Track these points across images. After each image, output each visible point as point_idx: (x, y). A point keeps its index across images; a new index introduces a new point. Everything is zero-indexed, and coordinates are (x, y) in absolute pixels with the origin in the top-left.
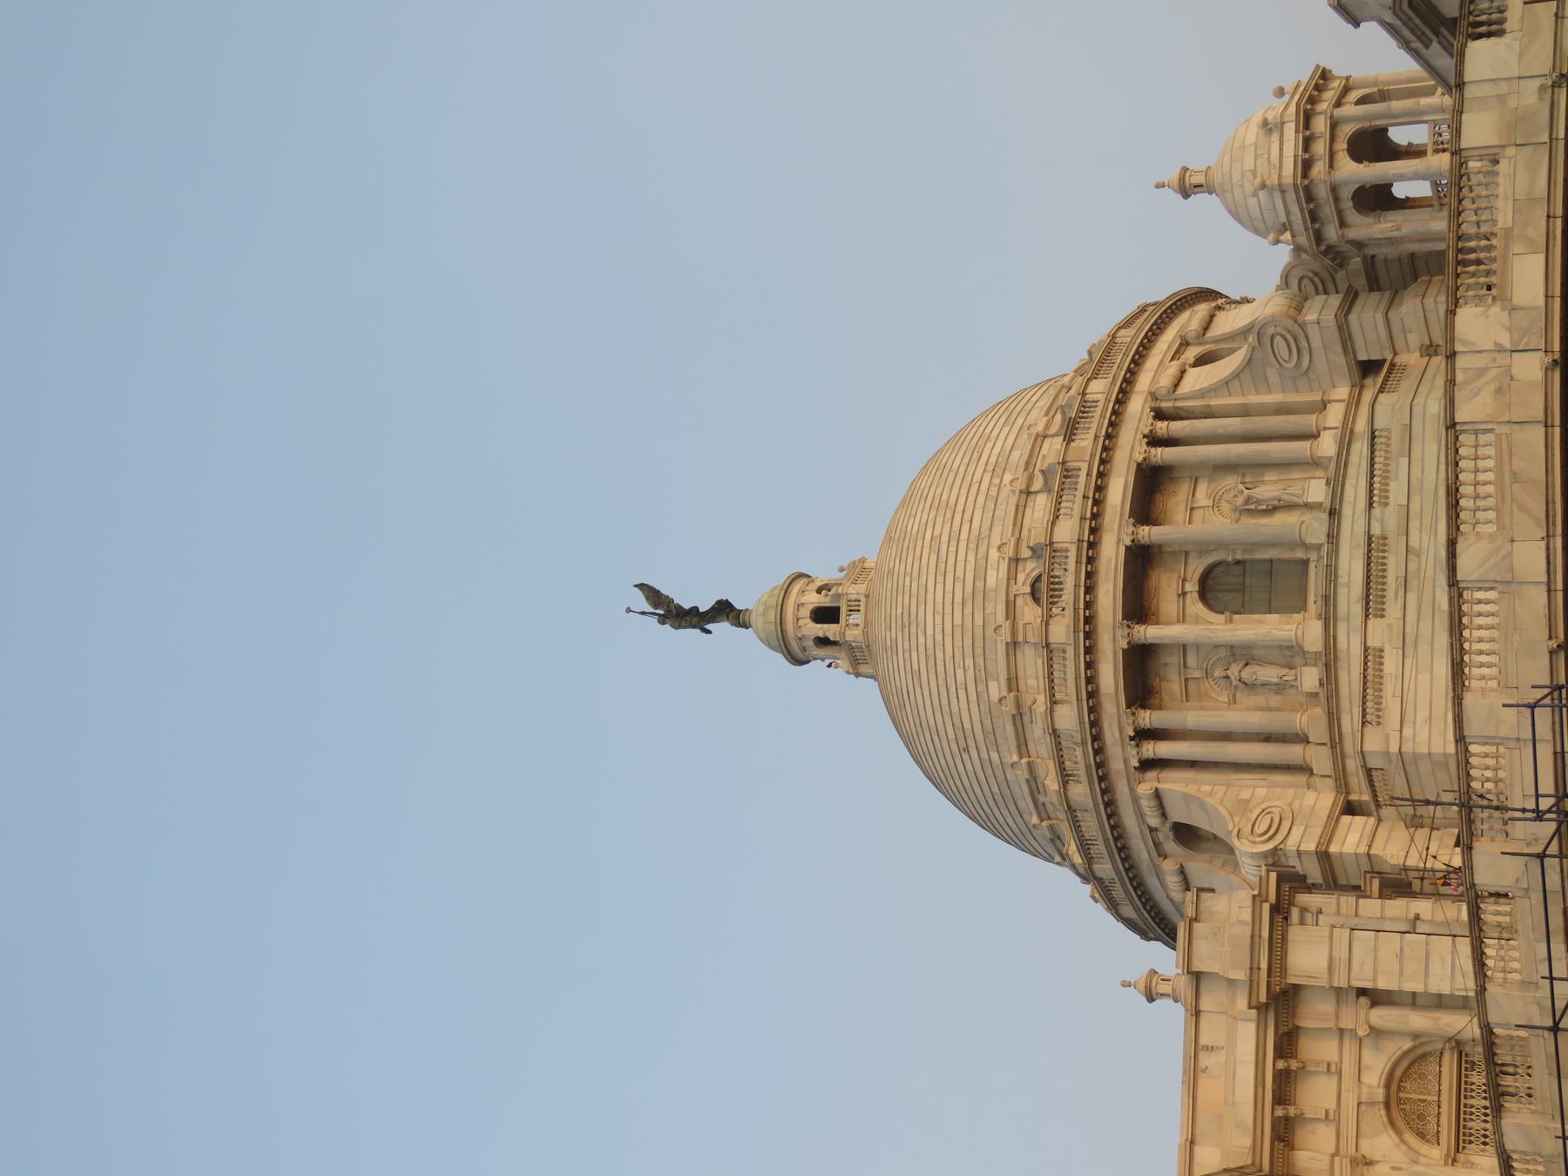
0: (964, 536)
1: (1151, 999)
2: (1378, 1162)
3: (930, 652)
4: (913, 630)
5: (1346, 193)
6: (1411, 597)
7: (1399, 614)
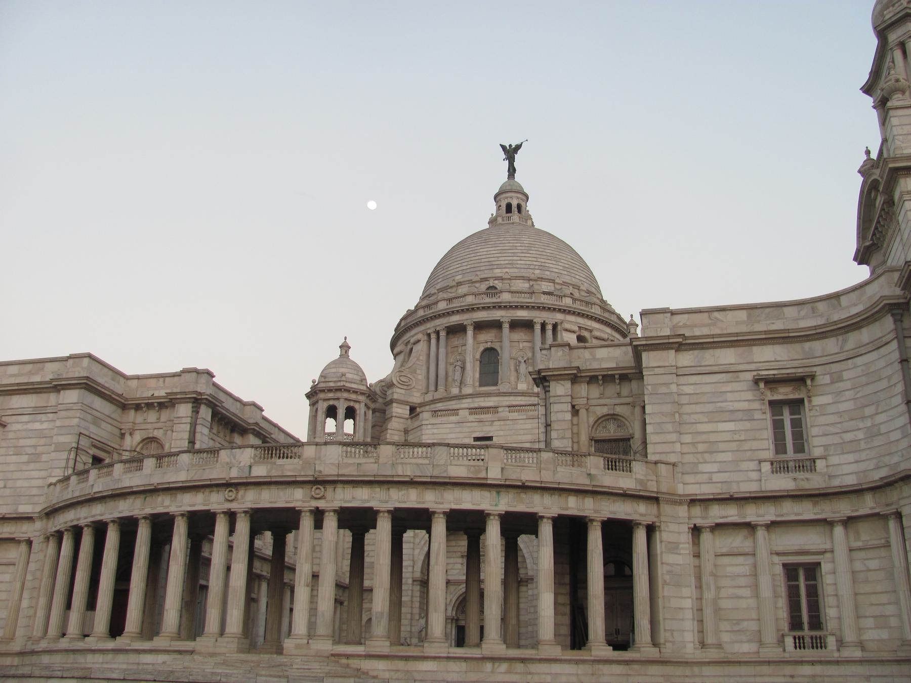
0: (515, 258)
1: (340, 347)
2: (132, 437)
3: (474, 252)
4: (483, 244)
6: (475, 424)
7: (470, 420)
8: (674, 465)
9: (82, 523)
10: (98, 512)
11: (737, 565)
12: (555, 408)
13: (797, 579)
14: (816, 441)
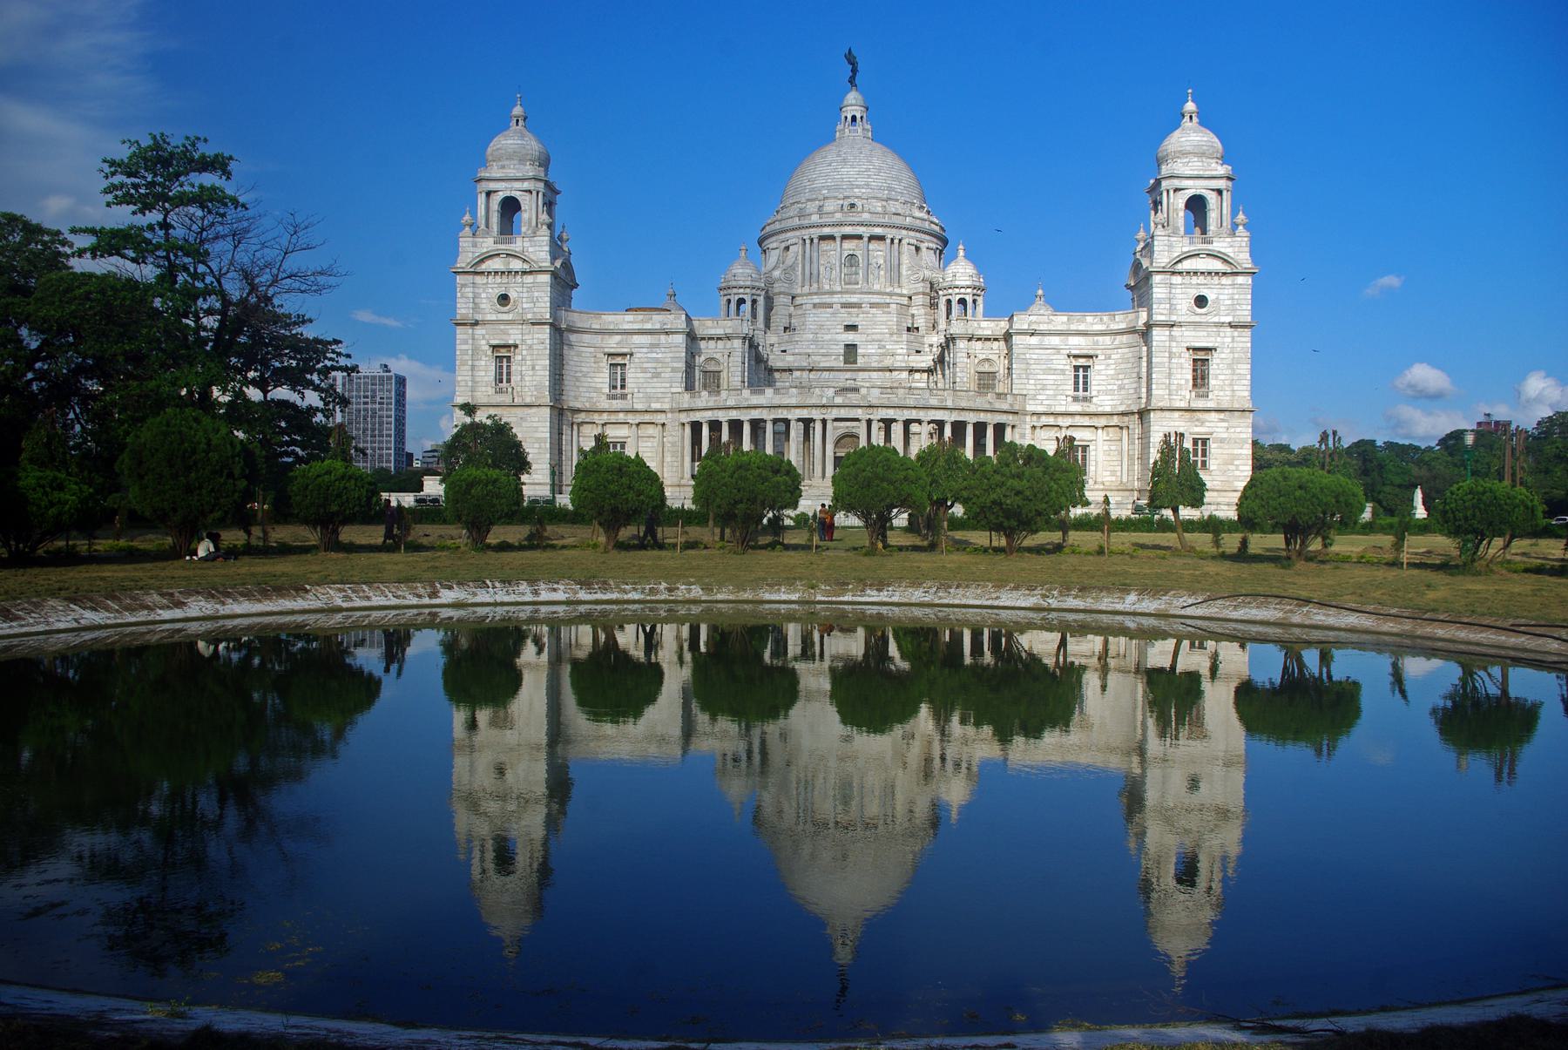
5: (950, 297)
9: (720, 419)
12: (959, 355)
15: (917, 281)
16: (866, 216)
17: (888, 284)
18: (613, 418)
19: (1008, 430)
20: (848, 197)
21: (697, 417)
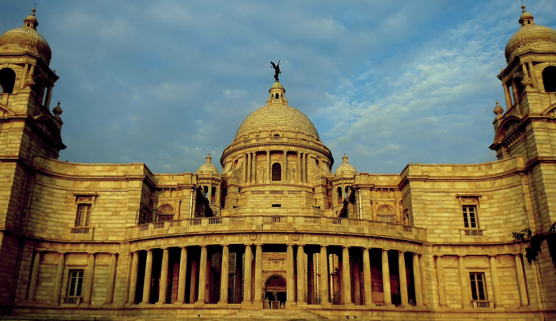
5: (340, 186)
6: (273, 198)
8: (425, 230)
9: (162, 247)
10: (173, 243)
11: (451, 272)
13: (474, 279)
14: (481, 223)
15: (318, 178)
16: (285, 140)
17: (300, 180)
18: (74, 249)
19: (416, 258)
20: (274, 131)
21: (143, 246)
